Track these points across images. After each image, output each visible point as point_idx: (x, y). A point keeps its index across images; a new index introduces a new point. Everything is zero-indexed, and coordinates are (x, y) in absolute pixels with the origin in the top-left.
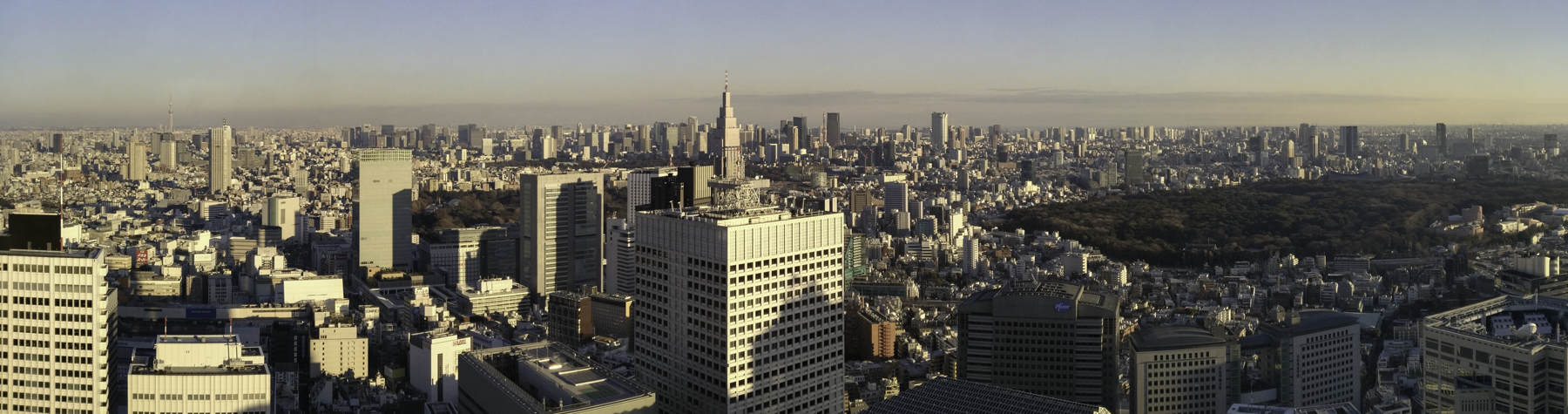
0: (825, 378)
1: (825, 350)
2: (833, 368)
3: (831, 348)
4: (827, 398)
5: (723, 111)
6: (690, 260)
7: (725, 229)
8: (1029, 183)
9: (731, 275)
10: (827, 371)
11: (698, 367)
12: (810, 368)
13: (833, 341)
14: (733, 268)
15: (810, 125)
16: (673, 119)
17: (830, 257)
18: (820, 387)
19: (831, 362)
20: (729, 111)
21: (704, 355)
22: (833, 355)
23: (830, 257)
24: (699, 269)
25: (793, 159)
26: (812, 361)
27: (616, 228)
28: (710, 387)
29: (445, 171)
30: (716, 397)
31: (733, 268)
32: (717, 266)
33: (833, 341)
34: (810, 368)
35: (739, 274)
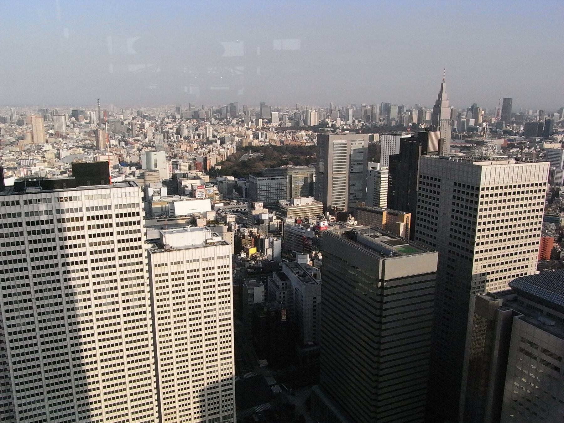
0: (527, 255)
1: (529, 240)
2: (532, 251)
3: (533, 240)
4: (527, 266)
5: (440, 95)
6: (455, 184)
7: (480, 167)
9: (481, 193)
11: (456, 242)
12: (519, 249)
13: (534, 236)
14: (483, 189)
16: (394, 102)
21: (461, 236)
22: (533, 244)
24: (461, 189)
25: (477, 130)
26: (521, 245)
28: (463, 253)
29: (250, 133)
30: (467, 258)
31: (483, 189)
32: (473, 188)
33: (534, 236)
34: (519, 249)
35: (486, 192)
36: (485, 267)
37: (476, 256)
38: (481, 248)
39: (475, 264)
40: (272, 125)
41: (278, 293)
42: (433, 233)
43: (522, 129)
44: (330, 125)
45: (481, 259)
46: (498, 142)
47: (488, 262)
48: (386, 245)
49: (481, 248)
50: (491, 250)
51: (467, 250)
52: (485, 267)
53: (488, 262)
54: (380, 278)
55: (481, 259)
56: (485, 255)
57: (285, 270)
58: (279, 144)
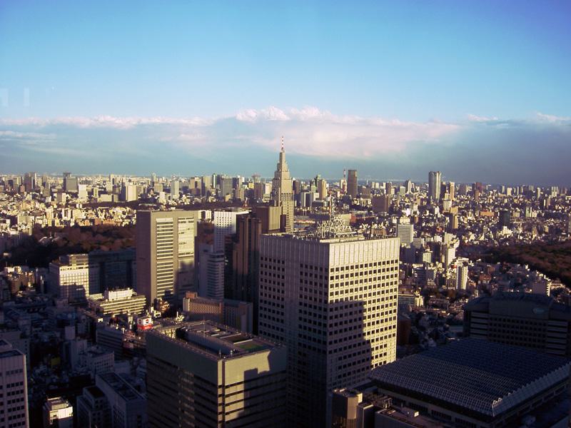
0: (384, 342)
3: (389, 324)
5: (280, 166)
6: (302, 266)
7: (328, 245)
8: (505, 227)
9: (331, 274)
11: (307, 333)
14: (332, 270)
17: (390, 266)
20: (284, 166)
21: (311, 325)
23: (390, 266)
25: (322, 204)
27: (206, 251)
31: (332, 270)
35: (335, 274)
36: (340, 359)
37: (329, 348)
38: (334, 337)
39: (329, 356)
40: (78, 201)
41: (90, 414)
42: (279, 325)
43: (369, 203)
45: (335, 351)
46: (345, 218)
48: (226, 343)
49: (334, 337)
52: (340, 359)
54: (220, 383)
55: (335, 351)
56: (340, 345)
57: (99, 383)
58: (88, 223)
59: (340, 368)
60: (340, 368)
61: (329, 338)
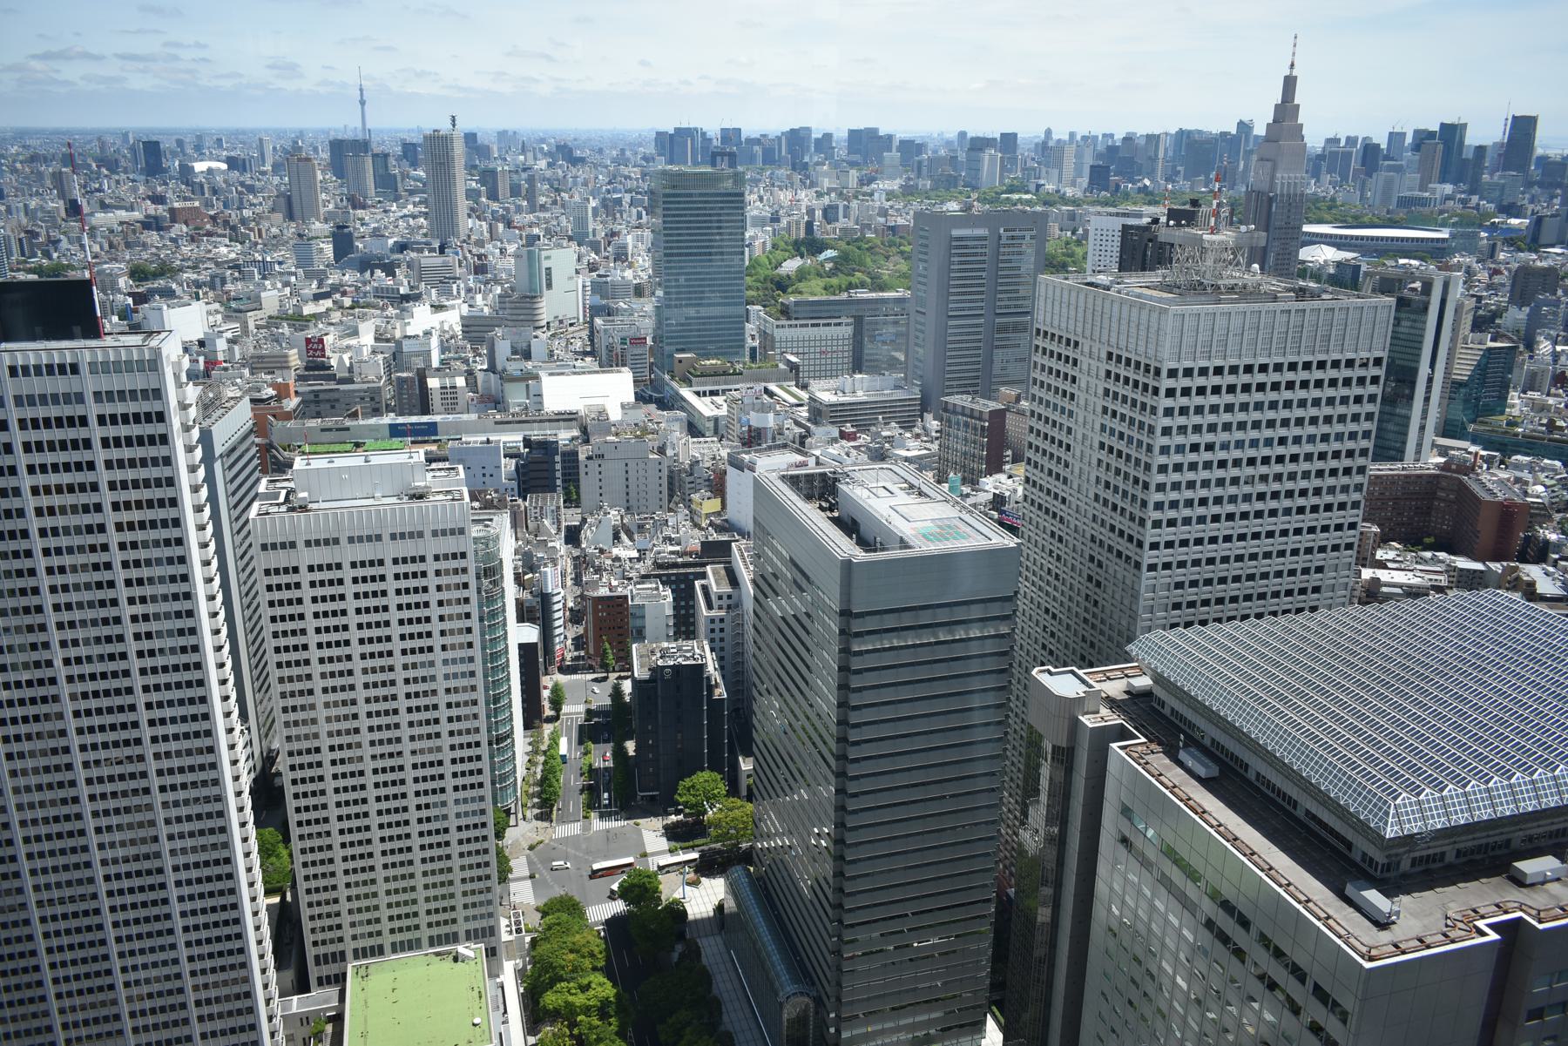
0: (1317, 559)
1: (1323, 518)
2: (1336, 548)
6: (1110, 355)
10: (1322, 549)
15: (1472, 138)
18: (1306, 571)
19: (1333, 537)
33: (1342, 506)
36: (1179, 585)
39: (1146, 574)
44: (1032, 188)
45: (1167, 566)
47: (1192, 573)
49: (1167, 534)
50: (1199, 542)
51: (1130, 538)
52: (1179, 585)
53: (1192, 573)
55: (1167, 566)
59: (1177, 606)
60: (1177, 606)
61: (1150, 535)
